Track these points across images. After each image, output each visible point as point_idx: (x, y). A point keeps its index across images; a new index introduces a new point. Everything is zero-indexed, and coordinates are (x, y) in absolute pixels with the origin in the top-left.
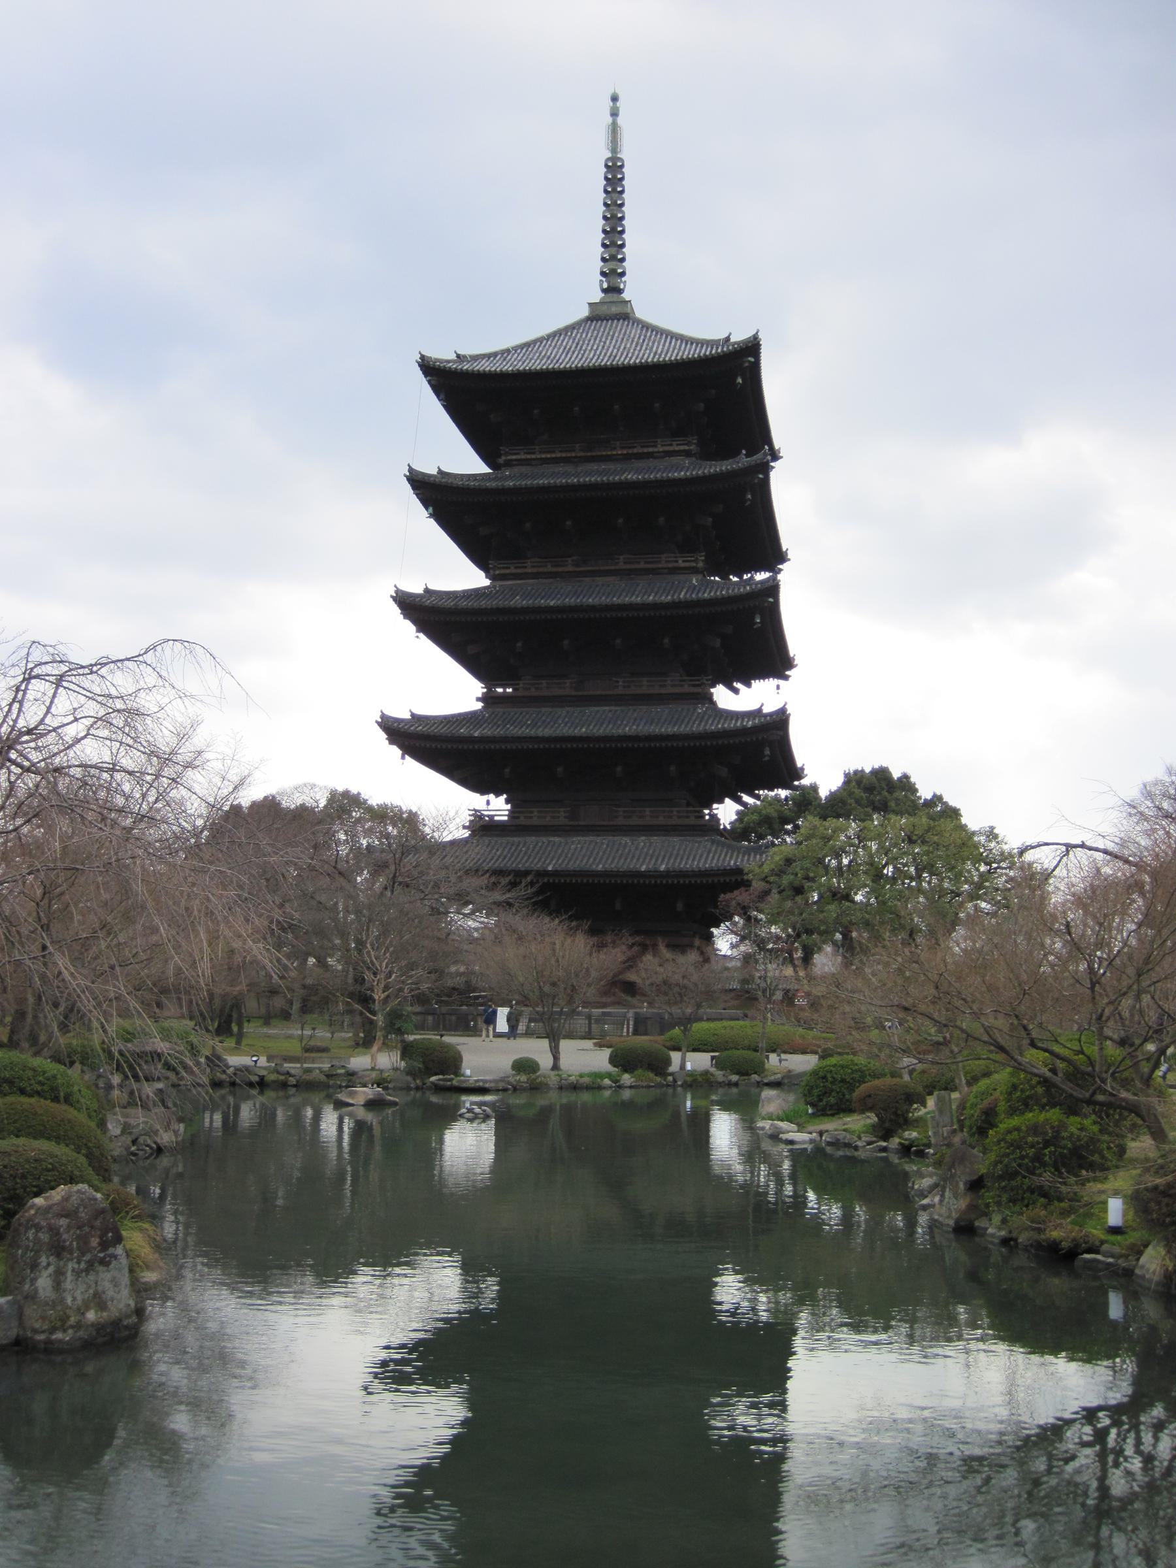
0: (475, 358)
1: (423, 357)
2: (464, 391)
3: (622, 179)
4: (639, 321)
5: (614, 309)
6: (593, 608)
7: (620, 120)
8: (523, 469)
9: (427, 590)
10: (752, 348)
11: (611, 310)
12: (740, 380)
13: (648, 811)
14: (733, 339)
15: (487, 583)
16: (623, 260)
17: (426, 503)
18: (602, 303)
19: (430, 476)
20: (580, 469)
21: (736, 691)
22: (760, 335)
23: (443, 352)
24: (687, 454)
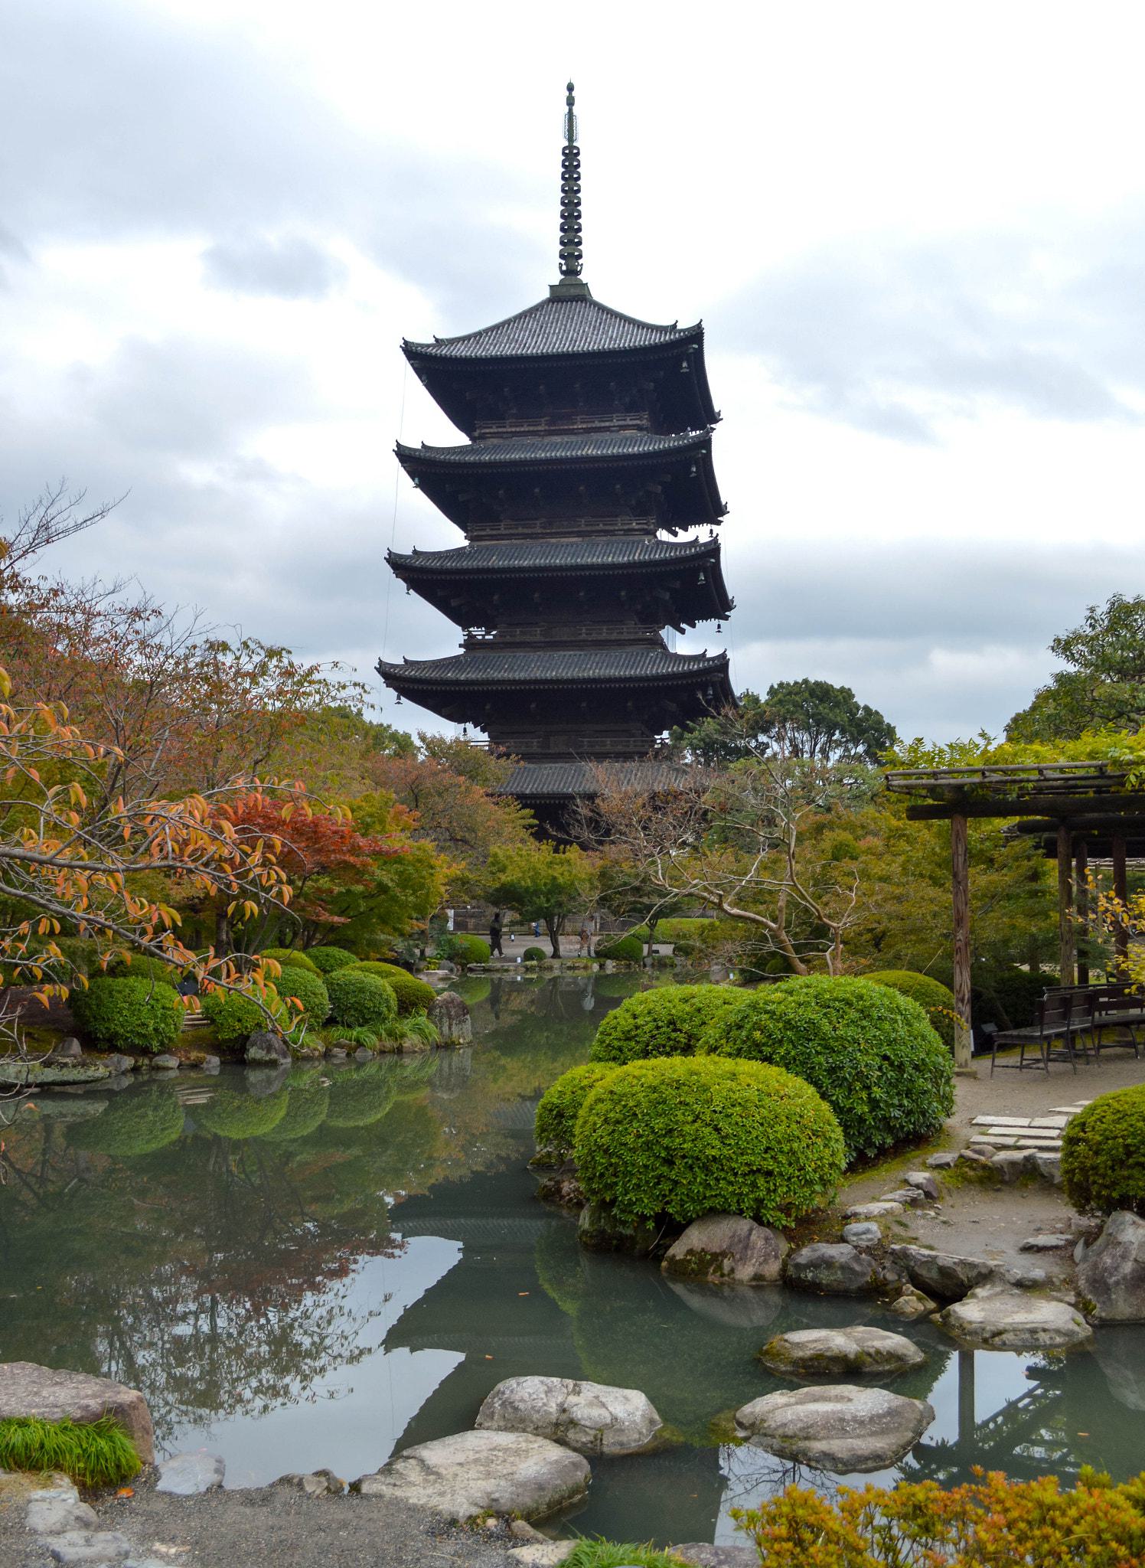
0: (452, 341)
1: (406, 342)
2: (441, 370)
3: (578, 166)
4: (596, 304)
5: (573, 291)
6: (560, 568)
7: (574, 108)
8: (495, 441)
9: (415, 552)
10: (696, 335)
11: (570, 293)
13: (608, 741)
14: (679, 327)
16: (580, 243)
17: (412, 475)
21: (683, 632)
22: (704, 325)
23: (423, 337)
24: (639, 428)
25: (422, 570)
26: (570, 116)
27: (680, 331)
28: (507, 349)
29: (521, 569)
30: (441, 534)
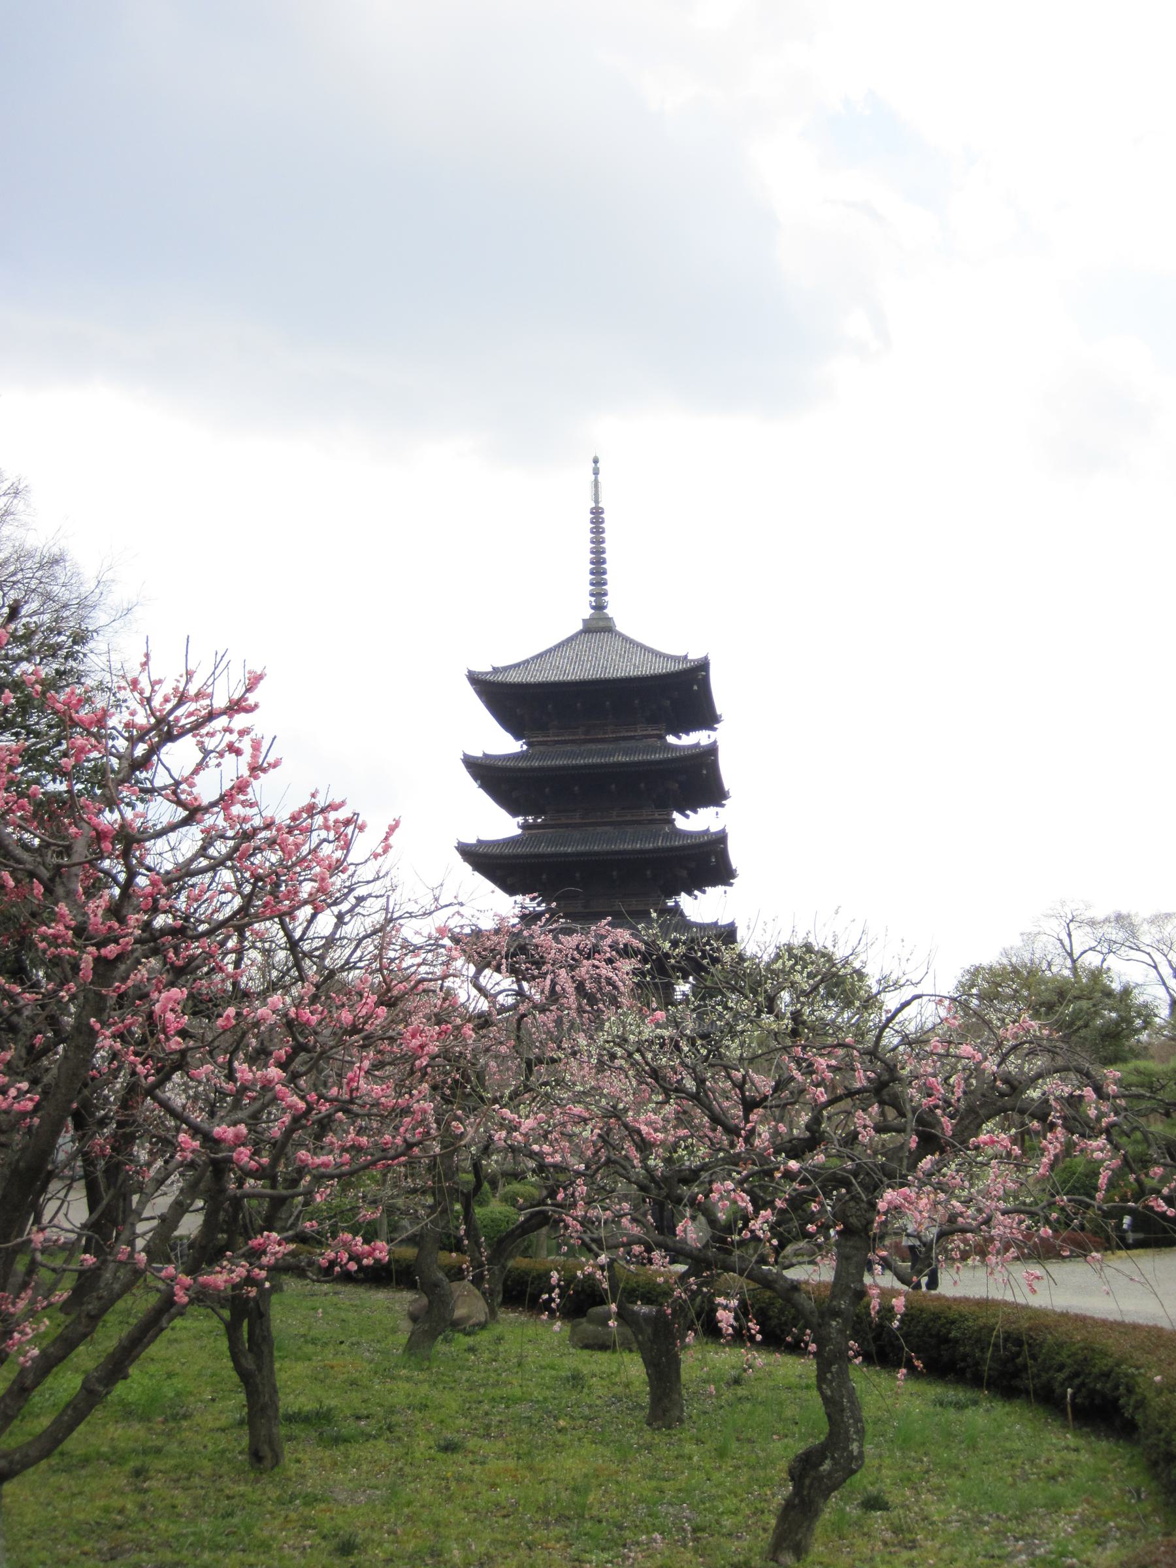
1: (469, 672)
4: (620, 635)
5: (601, 624)
6: (597, 853)
7: (599, 477)
9: (479, 841)
10: (703, 667)
11: (599, 625)
12: (695, 688)
15: (519, 831)
17: (476, 779)
18: (592, 619)
19: (477, 758)
20: (582, 748)
23: (483, 666)
25: (485, 856)
26: (596, 484)
27: (691, 661)
28: (552, 676)
29: (566, 855)
30: (500, 825)
